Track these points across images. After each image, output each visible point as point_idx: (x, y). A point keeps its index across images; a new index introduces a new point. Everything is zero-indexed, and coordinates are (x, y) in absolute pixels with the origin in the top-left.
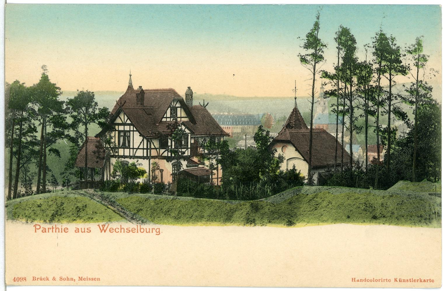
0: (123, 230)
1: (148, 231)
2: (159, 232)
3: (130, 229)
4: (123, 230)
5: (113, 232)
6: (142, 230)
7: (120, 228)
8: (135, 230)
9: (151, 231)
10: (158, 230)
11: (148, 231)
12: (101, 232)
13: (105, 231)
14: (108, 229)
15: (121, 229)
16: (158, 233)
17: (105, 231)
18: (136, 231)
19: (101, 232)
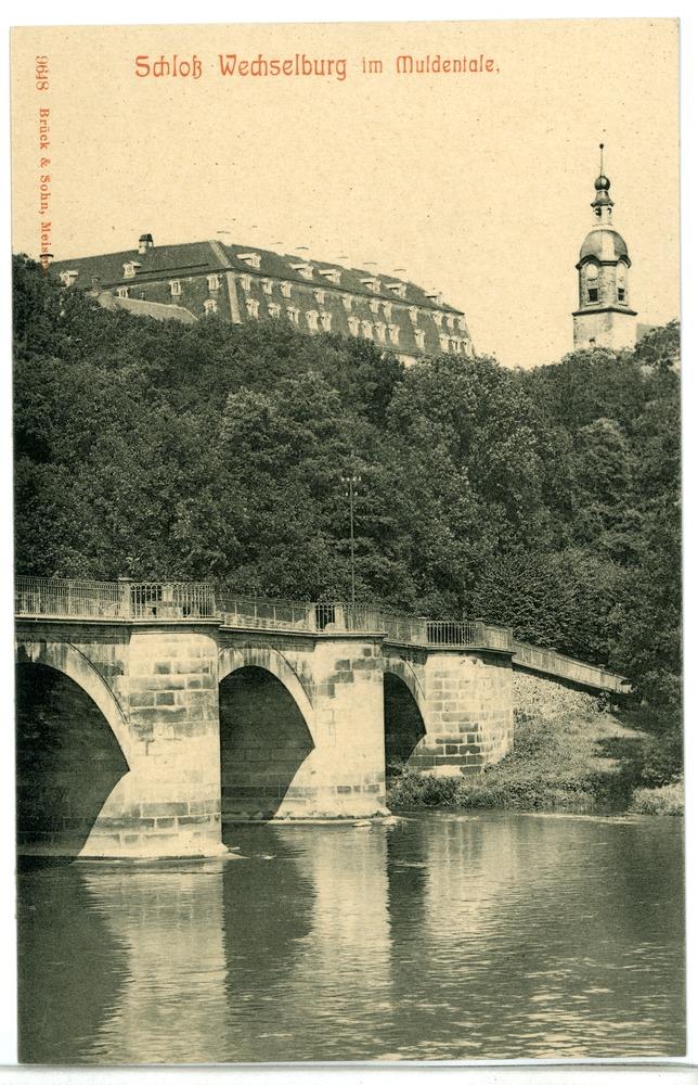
2: (344, 72)
3: (280, 65)
6: (307, 65)
12: (224, 73)
14: (236, 69)
17: (231, 73)
18: (294, 72)
19: (224, 73)
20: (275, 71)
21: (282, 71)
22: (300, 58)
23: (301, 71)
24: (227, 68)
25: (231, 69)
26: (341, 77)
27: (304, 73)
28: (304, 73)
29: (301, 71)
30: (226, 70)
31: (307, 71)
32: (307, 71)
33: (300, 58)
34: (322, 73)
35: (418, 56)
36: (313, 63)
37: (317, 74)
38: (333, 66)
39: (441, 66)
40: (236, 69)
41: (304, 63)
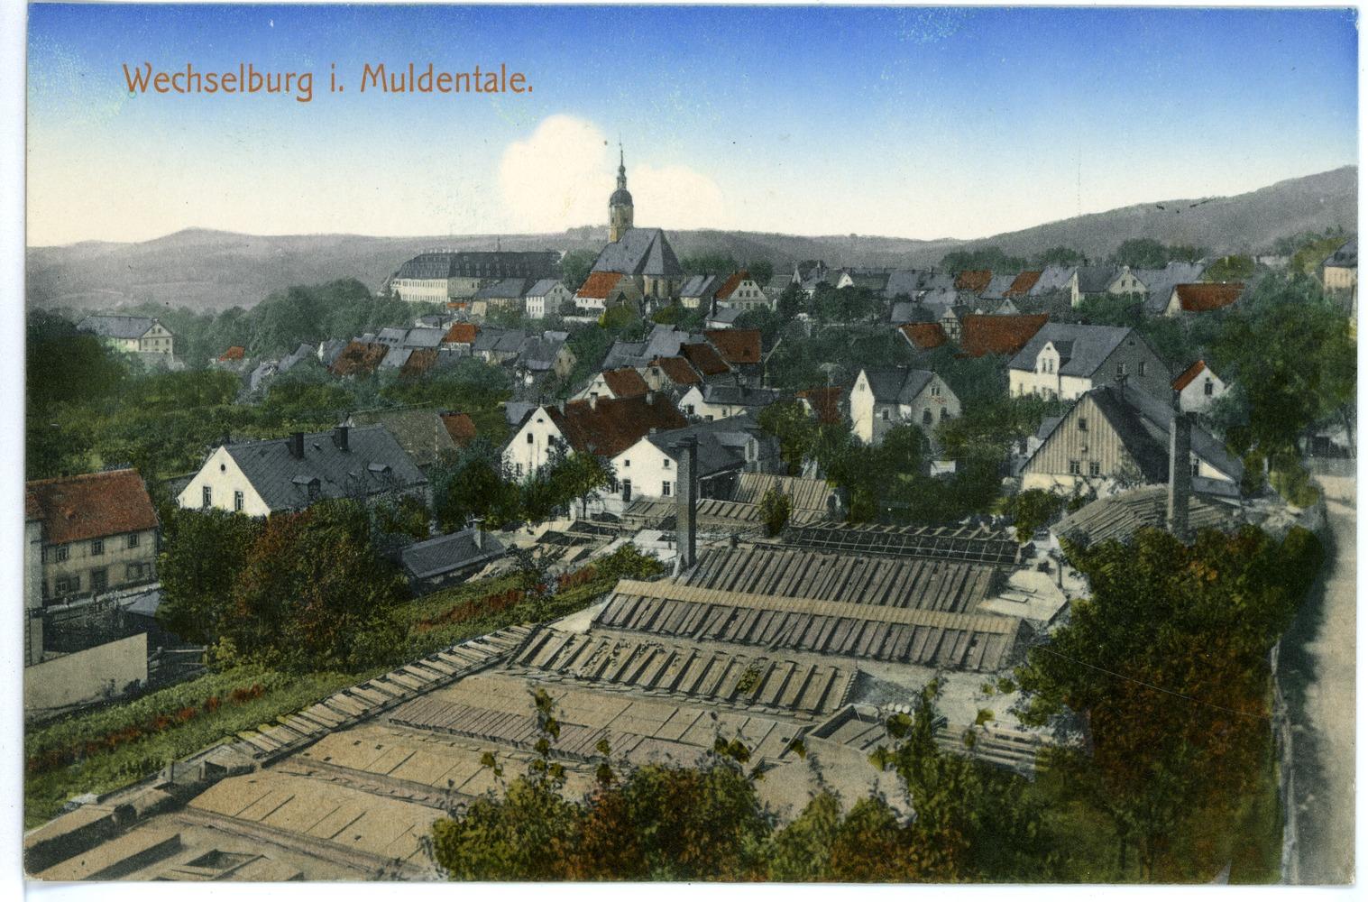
0: (194, 80)
1: (274, 85)
2: (309, 89)
4: (194, 80)
5: (167, 90)
7: (184, 70)
10: (305, 84)
12: (132, 89)
13: (143, 89)
14: (151, 81)
15: (190, 77)
17: (143, 89)
19: (132, 89)
20: (211, 87)
21: (220, 87)
22: (246, 70)
23: (246, 87)
24: (138, 76)
25: (143, 79)
26: (305, 95)
28: (251, 90)
29: (246, 87)
31: (255, 85)
33: (246, 70)
34: (278, 89)
36: (265, 77)
38: (293, 83)
40: (151, 81)
41: (251, 75)
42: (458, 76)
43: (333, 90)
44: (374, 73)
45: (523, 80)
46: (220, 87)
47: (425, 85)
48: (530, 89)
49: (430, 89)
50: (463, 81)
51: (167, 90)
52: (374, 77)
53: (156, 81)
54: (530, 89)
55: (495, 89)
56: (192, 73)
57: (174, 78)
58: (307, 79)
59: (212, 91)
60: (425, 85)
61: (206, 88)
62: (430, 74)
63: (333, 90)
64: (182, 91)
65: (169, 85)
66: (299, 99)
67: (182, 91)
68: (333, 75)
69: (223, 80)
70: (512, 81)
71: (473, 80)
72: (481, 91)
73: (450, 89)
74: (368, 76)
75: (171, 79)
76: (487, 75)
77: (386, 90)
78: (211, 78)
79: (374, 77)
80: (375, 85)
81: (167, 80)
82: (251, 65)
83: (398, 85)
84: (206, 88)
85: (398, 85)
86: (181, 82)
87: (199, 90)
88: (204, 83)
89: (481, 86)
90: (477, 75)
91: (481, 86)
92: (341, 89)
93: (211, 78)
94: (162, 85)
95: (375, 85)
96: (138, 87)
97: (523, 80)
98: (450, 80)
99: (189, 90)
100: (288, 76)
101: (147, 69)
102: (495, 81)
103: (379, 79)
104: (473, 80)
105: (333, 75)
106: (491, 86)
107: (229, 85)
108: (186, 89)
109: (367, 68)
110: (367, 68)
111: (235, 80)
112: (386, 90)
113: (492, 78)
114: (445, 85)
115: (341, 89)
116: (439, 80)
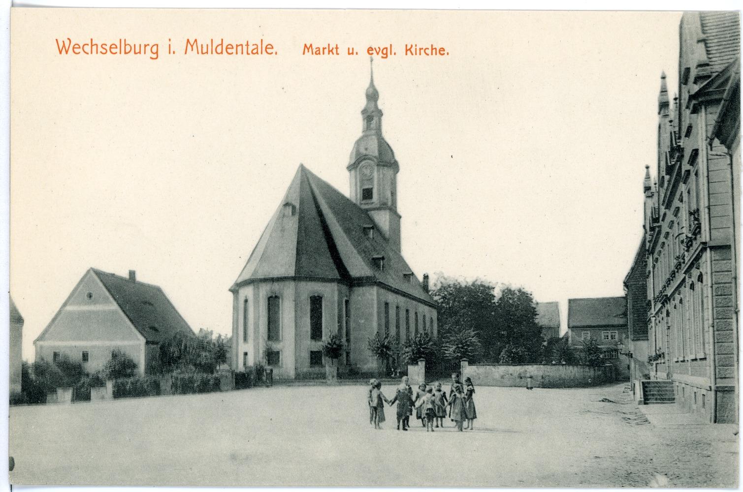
0: (94, 48)
1: (137, 51)
2: (157, 53)
3: (108, 48)
4: (94, 48)
5: (79, 53)
7: (430, 48)
8: (116, 48)
9: (142, 51)
10: (154, 50)
11: (137, 51)
12: (61, 53)
13: (67, 52)
15: (432, 49)
16: (155, 56)
17: (67, 52)
19: (61, 53)
20: (104, 51)
25: (67, 48)
26: (155, 56)
27: (126, 53)
28: (126, 53)
30: (62, 49)
31: (127, 50)
32: (127, 51)
34: (140, 52)
35: (204, 41)
37: (135, 53)
38: (148, 48)
39: (227, 49)
41: (125, 45)
42: (237, 46)
43: (170, 53)
44: (192, 44)
45: (272, 48)
46: (381, 49)
47: (219, 50)
48: (276, 53)
49: (222, 53)
50: (240, 48)
51: (79, 53)
52: (192, 46)
53: (74, 48)
54: (276, 53)
55: (257, 53)
56: (433, 48)
57: (425, 50)
58: (155, 47)
59: (104, 54)
60: (219, 50)
61: (101, 52)
62: (222, 44)
63: (170, 53)
64: (88, 53)
65: (81, 50)
66: (151, 58)
67: (88, 54)
68: (170, 45)
69: (111, 48)
70: (266, 48)
71: (245, 48)
72: (249, 54)
73: (116, 53)
74: (189, 45)
75: (81, 47)
76: (316, 48)
77: (198, 53)
78: (104, 46)
79: (192, 46)
80: (192, 50)
81: (80, 48)
82: (125, 40)
83: (205, 50)
84: (101, 52)
85: (205, 50)
86: (88, 49)
87: (97, 53)
88: (100, 49)
89: (250, 52)
90: (247, 45)
91: (250, 52)
92: (174, 53)
93: (104, 46)
94: (77, 50)
95: (192, 50)
96: (64, 51)
97: (272, 48)
98: (233, 48)
99: (92, 53)
100: (145, 46)
101: (68, 41)
102: (257, 48)
103: (195, 47)
104: (245, 48)
105: (170, 45)
106: (255, 51)
107: (114, 51)
108: (90, 53)
109: (188, 41)
110: (188, 41)
111: (116, 48)
112: (198, 53)
113: (255, 47)
114: (114, 51)
115: (174, 53)
116: (227, 48)
